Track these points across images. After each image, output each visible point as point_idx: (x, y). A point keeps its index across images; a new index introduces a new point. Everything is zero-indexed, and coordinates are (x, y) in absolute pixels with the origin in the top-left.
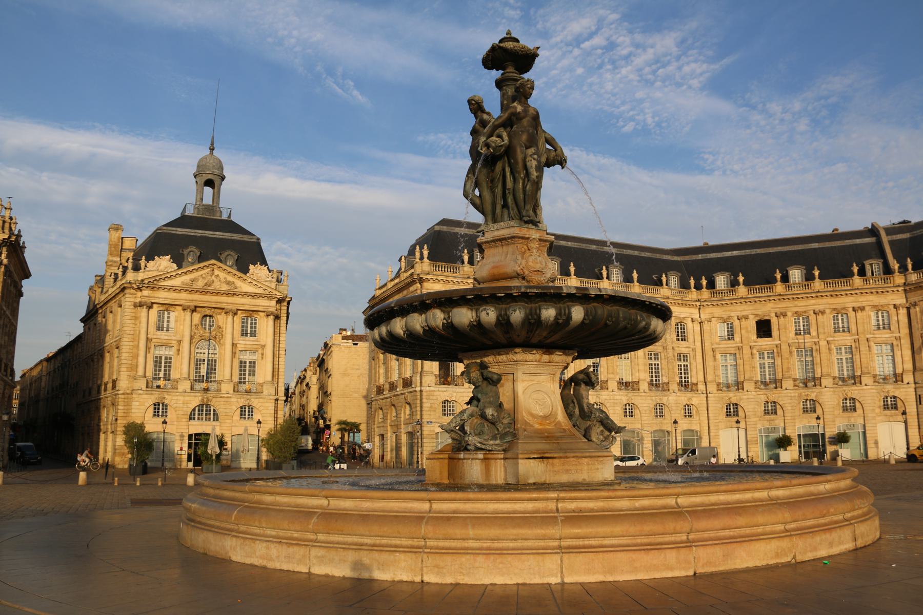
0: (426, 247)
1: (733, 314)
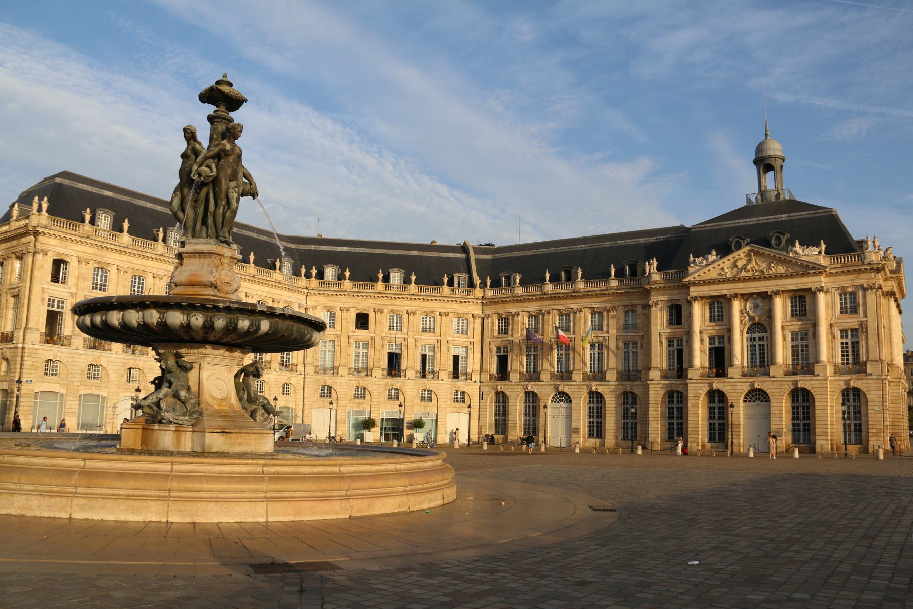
0: (46, 199)
1: (336, 304)
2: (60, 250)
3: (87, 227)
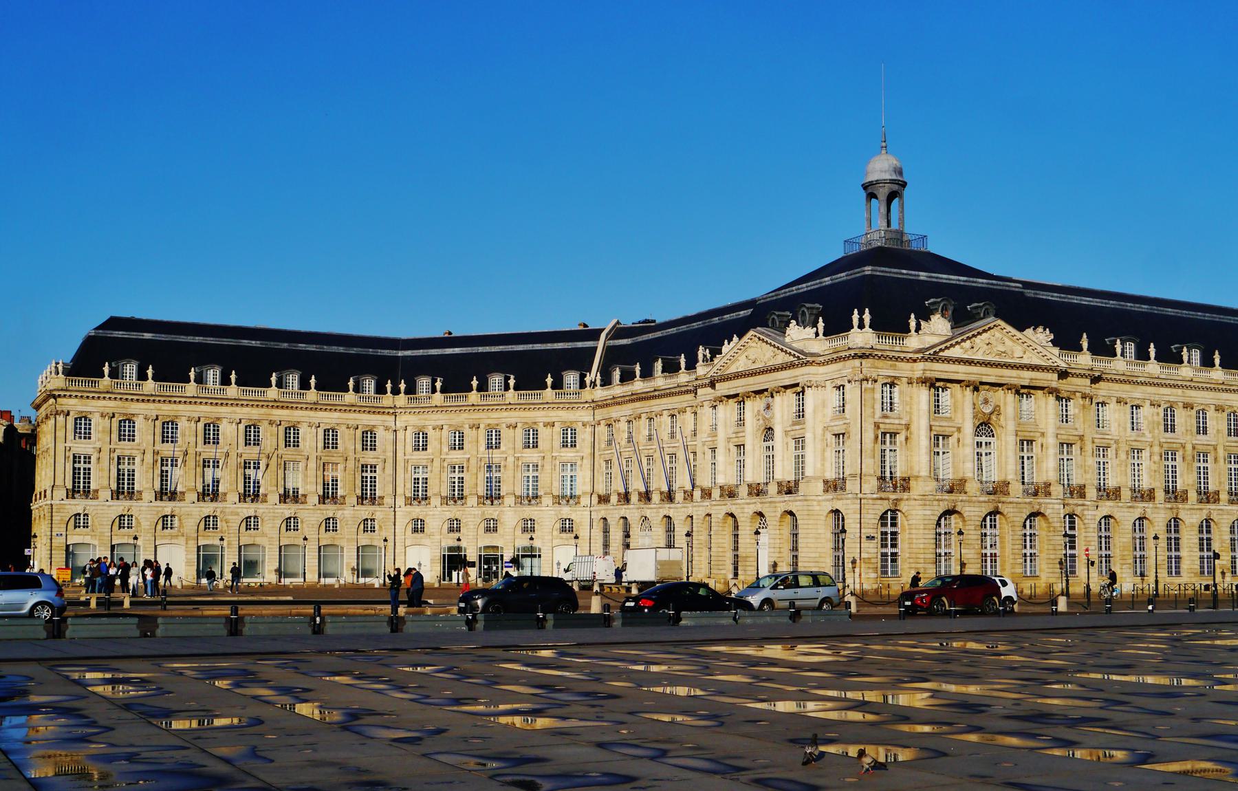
1: (427, 423)
2: (80, 408)
3: (106, 382)
